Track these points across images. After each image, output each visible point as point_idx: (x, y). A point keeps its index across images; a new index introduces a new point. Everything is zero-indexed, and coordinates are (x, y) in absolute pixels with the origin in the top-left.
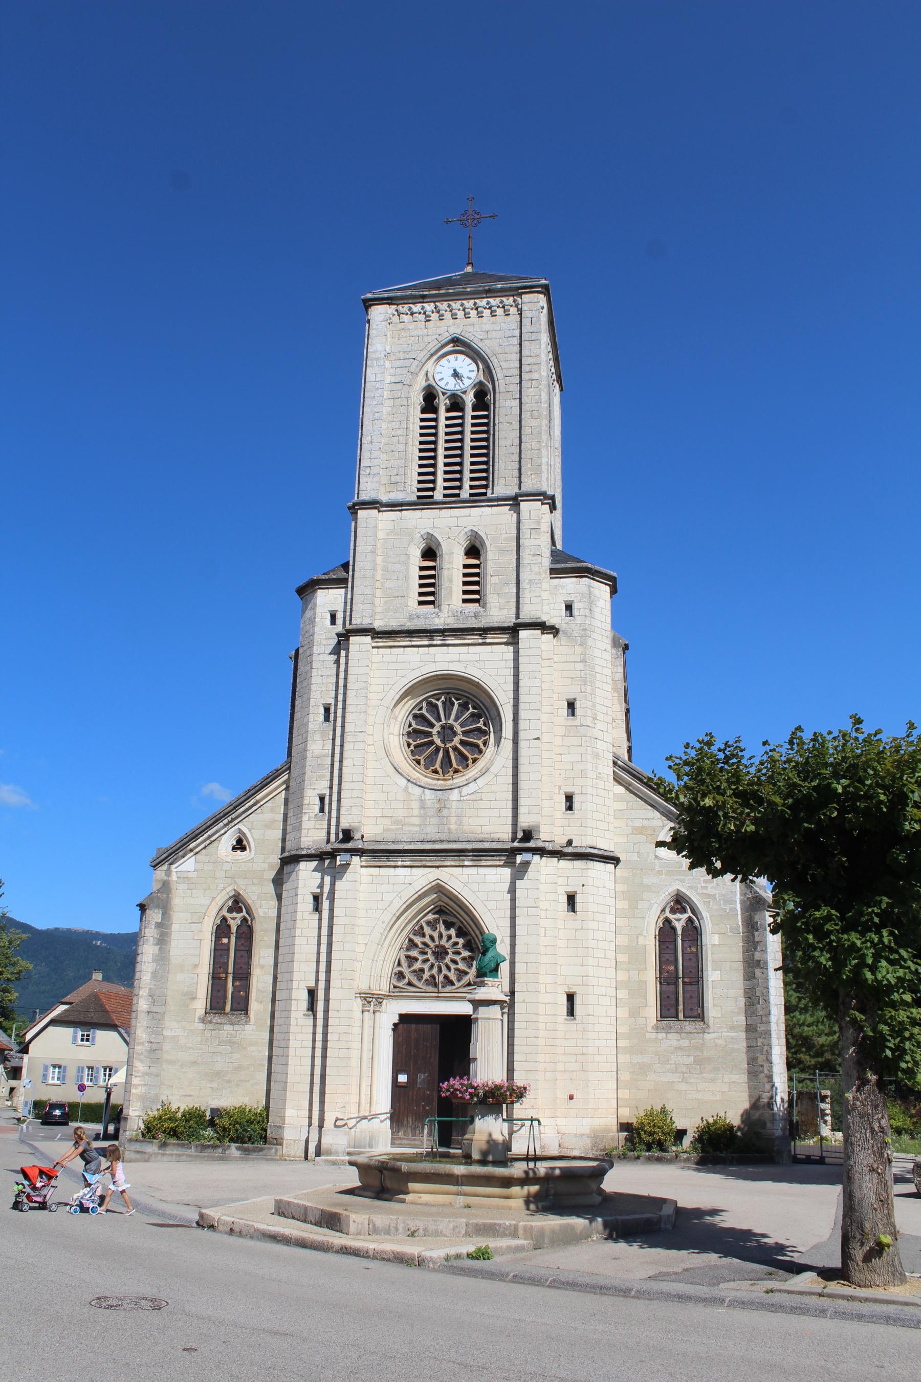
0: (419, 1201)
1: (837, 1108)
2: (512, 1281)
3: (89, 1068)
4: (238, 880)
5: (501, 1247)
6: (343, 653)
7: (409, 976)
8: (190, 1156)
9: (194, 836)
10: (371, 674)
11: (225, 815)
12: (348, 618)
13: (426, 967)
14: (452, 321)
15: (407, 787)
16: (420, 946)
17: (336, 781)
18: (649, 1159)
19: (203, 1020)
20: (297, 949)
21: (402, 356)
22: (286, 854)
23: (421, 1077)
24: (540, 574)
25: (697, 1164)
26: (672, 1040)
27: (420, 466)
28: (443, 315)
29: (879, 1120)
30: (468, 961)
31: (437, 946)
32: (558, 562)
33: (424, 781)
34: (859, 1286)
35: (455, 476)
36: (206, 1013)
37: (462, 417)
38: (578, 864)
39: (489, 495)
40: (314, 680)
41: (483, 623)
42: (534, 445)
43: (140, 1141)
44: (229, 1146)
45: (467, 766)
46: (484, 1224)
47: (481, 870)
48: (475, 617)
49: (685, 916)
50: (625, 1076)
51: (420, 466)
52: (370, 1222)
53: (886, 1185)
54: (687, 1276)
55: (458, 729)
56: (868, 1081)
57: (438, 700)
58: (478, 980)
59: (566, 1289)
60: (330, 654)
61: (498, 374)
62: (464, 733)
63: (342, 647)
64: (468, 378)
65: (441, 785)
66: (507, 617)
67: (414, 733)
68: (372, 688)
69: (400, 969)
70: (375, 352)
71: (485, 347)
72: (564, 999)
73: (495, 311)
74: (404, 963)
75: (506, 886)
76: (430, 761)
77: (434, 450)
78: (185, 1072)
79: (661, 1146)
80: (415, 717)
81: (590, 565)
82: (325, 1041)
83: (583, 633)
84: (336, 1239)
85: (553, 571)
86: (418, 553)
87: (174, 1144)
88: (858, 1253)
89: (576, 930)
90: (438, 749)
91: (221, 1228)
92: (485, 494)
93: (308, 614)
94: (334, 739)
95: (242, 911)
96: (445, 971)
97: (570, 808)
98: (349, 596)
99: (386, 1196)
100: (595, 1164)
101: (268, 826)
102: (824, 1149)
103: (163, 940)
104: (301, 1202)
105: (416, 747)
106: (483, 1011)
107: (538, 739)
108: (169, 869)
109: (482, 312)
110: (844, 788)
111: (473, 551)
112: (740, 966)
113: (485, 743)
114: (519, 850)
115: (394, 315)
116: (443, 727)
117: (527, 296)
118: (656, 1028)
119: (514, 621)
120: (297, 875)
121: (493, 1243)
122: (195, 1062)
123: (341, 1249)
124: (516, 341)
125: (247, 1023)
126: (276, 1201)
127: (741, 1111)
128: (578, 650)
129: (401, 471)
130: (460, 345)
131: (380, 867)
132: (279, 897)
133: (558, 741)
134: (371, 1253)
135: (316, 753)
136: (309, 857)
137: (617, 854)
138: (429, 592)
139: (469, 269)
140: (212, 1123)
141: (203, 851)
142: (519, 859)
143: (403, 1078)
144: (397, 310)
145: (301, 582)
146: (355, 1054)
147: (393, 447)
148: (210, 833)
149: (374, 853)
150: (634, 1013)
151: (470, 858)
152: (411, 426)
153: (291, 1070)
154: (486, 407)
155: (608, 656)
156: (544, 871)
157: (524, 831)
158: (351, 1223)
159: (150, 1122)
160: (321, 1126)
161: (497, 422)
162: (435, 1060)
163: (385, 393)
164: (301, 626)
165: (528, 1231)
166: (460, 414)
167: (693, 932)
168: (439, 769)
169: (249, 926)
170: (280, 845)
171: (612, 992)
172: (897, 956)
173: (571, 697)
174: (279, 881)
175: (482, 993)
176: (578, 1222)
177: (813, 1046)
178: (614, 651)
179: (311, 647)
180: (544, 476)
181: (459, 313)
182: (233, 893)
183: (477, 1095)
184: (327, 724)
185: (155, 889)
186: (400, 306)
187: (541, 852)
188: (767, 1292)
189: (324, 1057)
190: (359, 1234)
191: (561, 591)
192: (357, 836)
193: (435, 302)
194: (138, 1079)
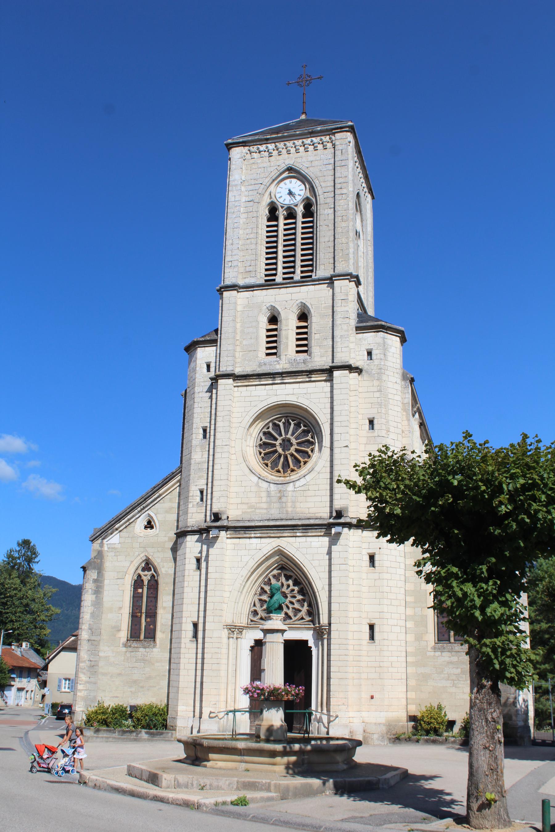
2: (250, 820)
3: (66, 679)
4: (147, 549)
6: (214, 391)
8: (114, 738)
9: (118, 519)
10: (234, 405)
12: (217, 367)
14: (287, 155)
15: (257, 484)
17: (210, 480)
18: (427, 741)
19: (125, 645)
21: (253, 182)
22: (179, 531)
24: (348, 331)
25: (461, 745)
28: (280, 152)
29: (492, 713)
34: (475, 828)
35: (290, 265)
36: (127, 640)
37: (295, 223)
39: (314, 277)
40: (196, 410)
42: (344, 240)
44: (141, 731)
45: (300, 466)
46: (249, 782)
47: (308, 539)
48: (304, 363)
51: (267, 259)
52: (175, 779)
53: (496, 758)
55: (294, 441)
57: (280, 421)
59: (281, 826)
60: (207, 392)
61: (319, 191)
62: (298, 444)
63: (214, 387)
65: (282, 481)
67: (264, 445)
69: (255, 608)
70: (234, 181)
71: (309, 172)
72: (368, 627)
73: (317, 147)
74: (258, 605)
75: (326, 550)
77: (276, 247)
78: (113, 681)
80: (265, 433)
81: (383, 323)
83: (379, 371)
84: (152, 790)
85: (358, 329)
87: (104, 730)
88: (475, 806)
89: (375, 580)
90: (280, 456)
91: (90, 784)
92: (311, 276)
93: (192, 365)
94: (209, 451)
95: (151, 570)
98: (218, 352)
99: (197, 763)
101: (168, 511)
103: (98, 591)
105: (265, 454)
106: (270, 637)
107: (347, 446)
108: (102, 543)
109: (308, 148)
110: (459, 482)
111: (303, 316)
113: (312, 451)
115: (247, 154)
116: (283, 440)
117: (339, 134)
118: (434, 649)
119: (331, 364)
120: (185, 545)
121: (249, 795)
122: (120, 674)
123: (154, 797)
124: (331, 167)
125: (154, 646)
126: (128, 766)
128: (376, 383)
129: (253, 263)
130: (293, 172)
131: (239, 538)
132: (175, 559)
134: (170, 800)
135: (198, 460)
136: (193, 532)
138: (273, 346)
139: (303, 117)
140: (131, 716)
141: (125, 530)
142: (333, 531)
144: (249, 150)
146: (224, 667)
148: (129, 517)
149: (235, 529)
150: (419, 638)
151: (301, 531)
152: (260, 231)
153: (181, 679)
155: (398, 387)
157: (336, 511)
158: (163, 780)
159: (89, 715)
160: (200, 718)
161: (318, 225)
163: (242, 209)
165: (278, 787)
166: (293, 221)
170: (176, 524)
171: (402, 623)
172: (504, 599)
173: (371, 416)
174: (174, 549)
176: (316, 782)
178: (403, 383)
179: (194, 388)
180: (351, 261)
181: (292, 149)
182: (145, 558)
183: (264, 695)
185: (93, 556)
186: (251, 148)
187: (349, 525)
190: (168, 787)
191: (364, 342)
192: (224, 517)
193: (275, 143)
194: (82, 686)
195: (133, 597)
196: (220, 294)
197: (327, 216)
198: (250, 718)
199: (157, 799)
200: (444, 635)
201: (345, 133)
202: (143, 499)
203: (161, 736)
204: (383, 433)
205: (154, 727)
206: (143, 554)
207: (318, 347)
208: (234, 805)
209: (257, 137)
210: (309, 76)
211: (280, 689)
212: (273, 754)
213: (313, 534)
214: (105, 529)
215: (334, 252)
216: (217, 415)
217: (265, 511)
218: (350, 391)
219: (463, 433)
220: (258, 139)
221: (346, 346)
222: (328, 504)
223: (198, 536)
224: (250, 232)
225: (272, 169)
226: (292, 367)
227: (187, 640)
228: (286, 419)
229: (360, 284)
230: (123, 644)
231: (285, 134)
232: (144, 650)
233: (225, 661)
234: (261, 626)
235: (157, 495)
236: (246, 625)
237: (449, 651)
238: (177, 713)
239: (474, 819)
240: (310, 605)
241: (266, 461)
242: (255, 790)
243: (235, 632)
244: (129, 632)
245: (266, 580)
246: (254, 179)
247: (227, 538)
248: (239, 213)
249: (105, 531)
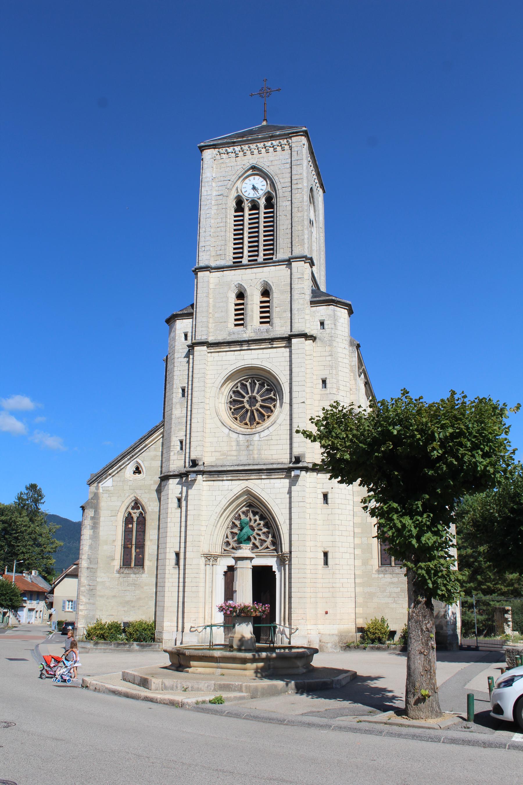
0: (196, 672)
1: (516, 617)
2: (226, 716)
3: (69, 601)
6: (191, 357)
9: (111, 466)
10: (208, 368)
11: (129, 453)
15: (229, 434)
18: (372, 648)
19: (118, 572)
20: (169, 529)
21: (222, 179)
22: (162, 475)
24: (304, 304)
25: (401, 651)
27: (235, 244)
28: (245, 153)
29: (426, 624)
30: (266, 534)
32: (315, 297)
35: (254, 249)
36: (120, 568)
37: (258, 214)
39: (274, 259)
40: (175, 373)
41: (271, 335)
42: (300, 228)
43: (85, 642)
44: (133, 644)
45: (264, 420)
46: (224, 685)
50: (360, 600)
53: (430, 661)
55: (259, 398)
56: (420, 602)
57: (247, 382)
59: (252, 720)
60: (185, 357)
61: (278, 186)
62: (263, 401)
64: (261, 190)
67: (233, 402)
68: (208, 377)
69: (227, 539)
72: (322, 555)
73: (276, 148)
74: (230, 536)
75: (287, 490)
76: (243, 418)
77: (242, 234)
80: (234, 392)
81: (334, 298)
83: (330, 338)
84: (143, 692)
85: (312, 303)
87: (102, 643)
88: (412, 701)
89: (328, 515)
90: (247, 411)
91: (91, 687)
92: (272, 259)
93: (172, 334)
94: (187, 407)
95: (139, 509)
98: (194, 323)
99: (180, 669)
100: (303, 650)
101: (153, 459)
103: (95, 527)
105: (234, 410)
106: (240, 564)
107: (304, 402)
108: (98, 486)
109: (269, 150)
110: (398, 431)
111: (266, 293)
113: (274, 406)
115: (217, 155)
116: (250, 398)
118: (378, 572)
119: (290, 333)
121: (225, 695)
122: (115, 596)
124: (288, 166)
125: (143, 573)
128: (328, 348)
130: (256, 170)
131: (214, 481)
132: (160, 499)
134: (158, 700)
135: (178, 416)
136: (174, 476)
138: (240, 318)
139: (264, 123)
140: (124, 631)
141: (117, 475)
142: (293, 474)
144: (219, 152)
145: (168, 316)
146: (201, 589)
148: (120, 464)
149: (210, 473)
150: (365, 563)
151: (265, 474)
152: (228, 221)
153: (166, 599)
155: (347, 352)
156: (308, 480)
157: (295, 457)
158: (153, 683)
159: (89, 631)
160: (183, 632)
161: (278, 215)
163: (213, 202)
165: (248, 688)
166: (257, 212)
171: (352, 550)
172: (436, 529)
173: (324, 377)
174: (159, 491)
175: (239, 553)
176: (280, 684)
177: (506, 580)
178: (351, 348)
180: (306, 246)
181: (255, 151)
182: (134, 498)
183: (236, 612)
184: (183, 398)
185: (90, 498)
186: (220, 150)
187: (306, 469)
188: (358, 722)
190: (157, 690)
192: (200, 463)
193: (240, 145)
194: (83, 606)
195: (125, 531)
197: (285, 207)
198: (224, 632)
199: (147, 699)
201: (300, 137)
204: (334, 391)
205: (144, 640)
206: (132, 496)
208: (212, 703)
209: (225, 141)
210: (269, 89)
211: (249, 607)
212: (244, 661)
215: (292, 238)
217: (235, 458)
219: (401, 390)
220: (226, 142)
224: (220, 221)
225: (238, 168)
230: (117, 571)
231: (249, 138)
233: (202, 584)
234: (232, 555)
235: (144, 445)
240: (274, 536)
241: (235, 416)
242: (229, 691)
243: (211, 560)
244: (122, 560)
245: (236, 516)
246: (223, 176)
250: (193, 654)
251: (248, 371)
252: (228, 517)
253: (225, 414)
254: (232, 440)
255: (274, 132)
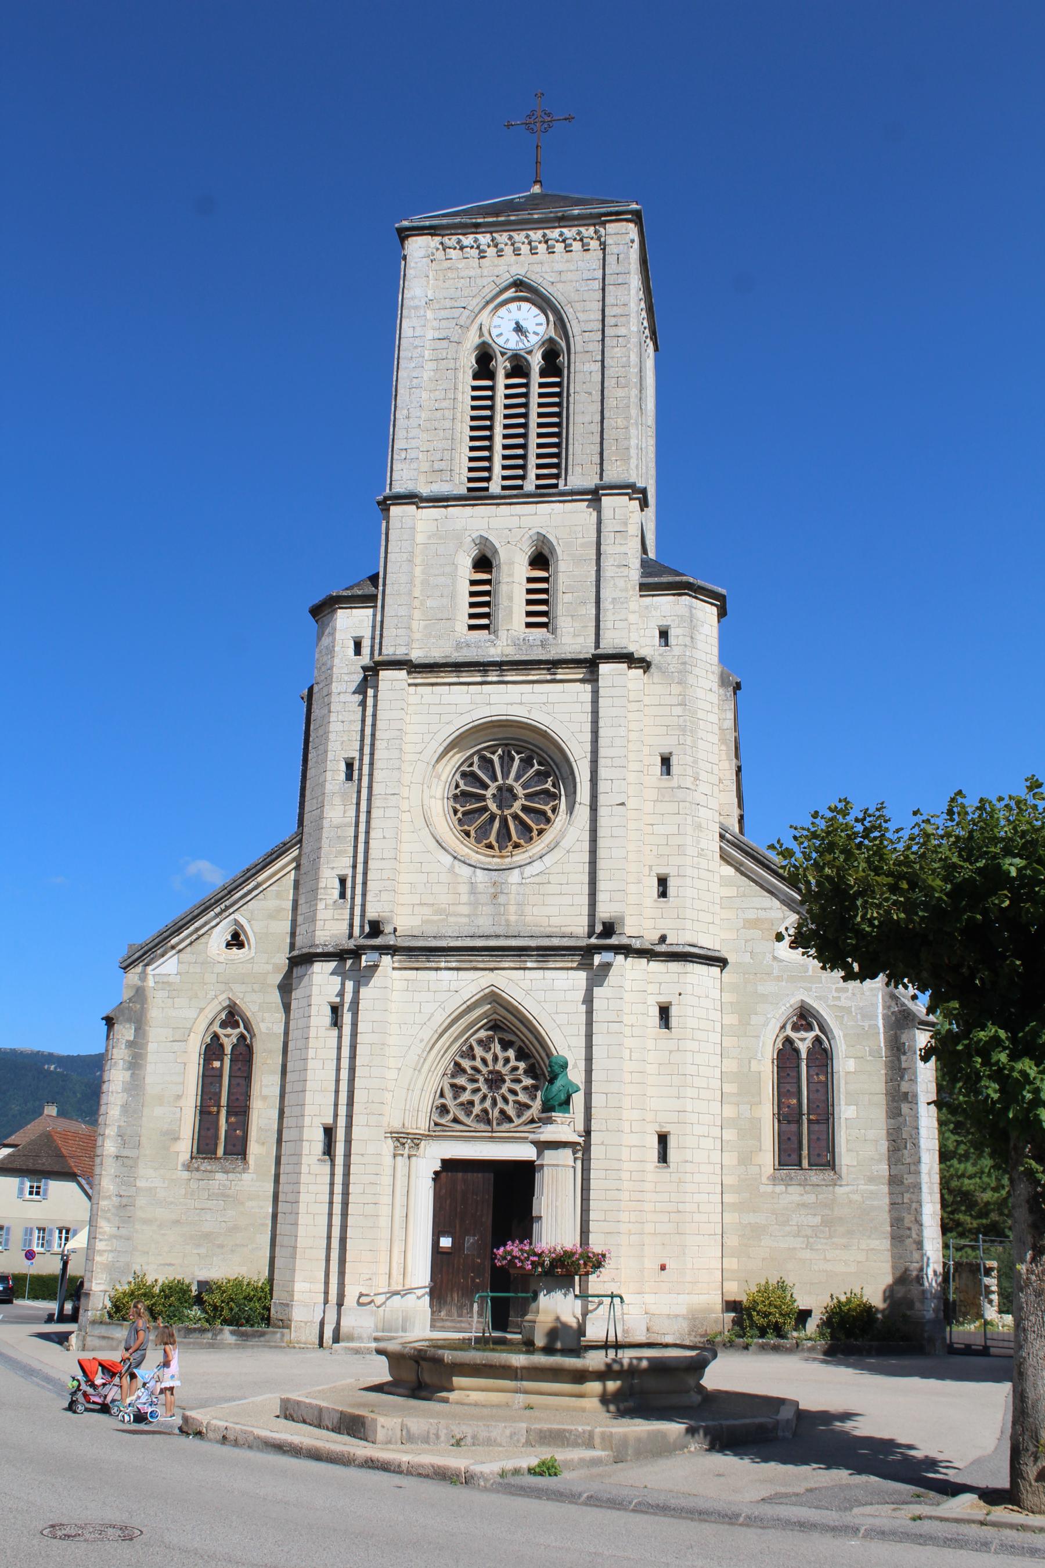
1: (1006, 1284)
2: (585, 1504)
3: (39, 1229)
5: (572, 1460)
6: (370, 692)
7: (454, 1110)
9: (177, 929)
10: (407, 719)
11: (218, 902)
12: (377, 647)
13: (477, 1098)
15: (453, 866)
16: (469, 1071)
18: (763, 1348)
19: (188, 1168)
20: (310, 1075)
21: (448, 303)
22: (296, 953)
23: (470, 1240)
24: (626, 590)
26: (794, 1194)
28: (502, 250)
30: (531, 1091)
31: (490, 1072)
33: (475, 858)
34: (1033, 1512)
35: (517, 462)
36: (192, 1158)
37: (526, 385)
38: (674, 966)
39: (561, 487)
40: (333, 727)
41: (552, 654)
43: (106, 1324)
44: (221, 1330)
45: (531, 839)
46: (550, 1431)
47: (548, 973)
49: (811, 1035)
50: (732, 1241)
54: (812, 1496)
55: (520, 791)
57: (493, 753)
58: (544, 1115)
59: (655, 1514)
60: (354, 693)
61: (575, 328)
66: (584, 647)
67: (462, 797)
69: (443, 1101)
70: (412, 298)
71: (557, 293)
73: (571, 245)
74: (449, 1093)
75: (581, 995)
78: (164, 1235)
79: (779, 1331)
80: (464, 775)
81: (691, 580)
82: (346, 1193)
83: (681, 667)
84: (360, 1449)
85: (643, 587)
86: (468, 562)
88: (1031, 1471)
89: (671, 1052)
91: (211, 1435)
92: (556, 486)
93: (325, 641)
94: (358, 804)
95: (238, 1026)
96: (500, 1104)
97: (663, 894)
98: (379, 618)
99: (424, 1394)
100: (693, 1353)
101: (273, 916)
102: (989, 1336)
103: (136, 1064)
104: (315, 1402)
105: (464, 814)
106: (550, 1157)
107: (623, 804)
108: (144, 972)
109: (554, 247)
110: (1019, 870)
111: (540, 560)
112: (882, 1100)
113: (554, 810)
114: (598, 946)
115: (438, 249)
116: (500, 789)
117: (613, 225)
118: (774, 1179)
119: (593, 651)
120: (310, 980)
121: (561, 1455)
123: (366, 1462)
124: (597, 285)
125: (245, 1170)
126: (282, 1400)
127: (883, 1287)
128: (676, 689)
129: (447, 455)
130: (524, 289)
131: (417, 969)
132: (287, 1008)
133: (649, 807)
134: (404, 1467)
135: (336, 821)
136: (326, 956)
137: (724, 954)
138: (483, 613)
139: (536, 189)
140: (199, 1300)
141: (189, 948)
142: (597, 959)
143: (446, 1242)
144: (442, 243)
145: (317, 599)
146: (385, 1210)
147: (436, 424)
148: (197, 925)
150: (745, 1159)
151: (534, 958)
152: (460, 397)
153: (301, 1231)
154: (558, 373)
155: (714, 698)
156: (629, 975)
157: (604, 924)
158: (379, 1428)
159: (118, 1299)
160: (340, 1304)
161: (572, 391)
162: (488, 1219)
164: (317, 656)
165: (607, 1440)
166: (524, 381)
167: (822, 1056)
168: (494, 843)
169: (248, 1046)
170: (288, 941)
173: (666, 750)
174: (286, 988)
175: (548, 1133)
176: (675, 1429)
177: (976, 1203)
179: (329, 685)
180: (633, 462)
181: (523, 247)
182: (227, 1003)
183: (542, 1265)
185: (126, 997)
186: (446, 239)
187: (626, 950)
188: (914, 1519)
189: (345, 1214)
190: (389, 1442)
191: (654, 613)
192: (388, 929)
193: (491, 233)
194: (104, 1243)
195: (204, 1075)
196: (382, 510)
198: (431, 1306)
199: (370, 1464)
200: (789, 1155)
201: (624, 223)
202: (226, 891)
203: (262, 1339)
204: (688, 782)
205: (247, 1322)
206: (224, 996)
207: (569, 618)
208: (535, 1474)
209: (458, 220)
210: (549, 115)
211: (575, 1253)
213: (558, 965)
214: (150, 946)
215: (602, 444)
216: (377, 737)
217: (465, 920)
218: (629, 702)
219: (1026, 780)
220: (461, 223)
221: (623, 618)
222: (585, 910)
223: (336, 963)
224: (442, 396)
226: (520, 652)
227: (313, 1160)
228: (506, 749)
229: (647, 506)
230: (183, 1165)
231: (513, 218)
232: (225, 1176)
234: (531, 1136)
236: (427, 1133)
237: (800, 1185)
238: (293, 1295)
239: (1030, 1496)
241: (466, 827)
242: (563, 1446)
243: (407, 1146)
245: (464, 1049)
247: (394, 969)
248: (421, 359)
249: (150, 950)
250: (463, 1361)
251: (496, 730)
252: (446, 1052)
253: (445, 826)
254: (460, 880)
255: (563, 209)
